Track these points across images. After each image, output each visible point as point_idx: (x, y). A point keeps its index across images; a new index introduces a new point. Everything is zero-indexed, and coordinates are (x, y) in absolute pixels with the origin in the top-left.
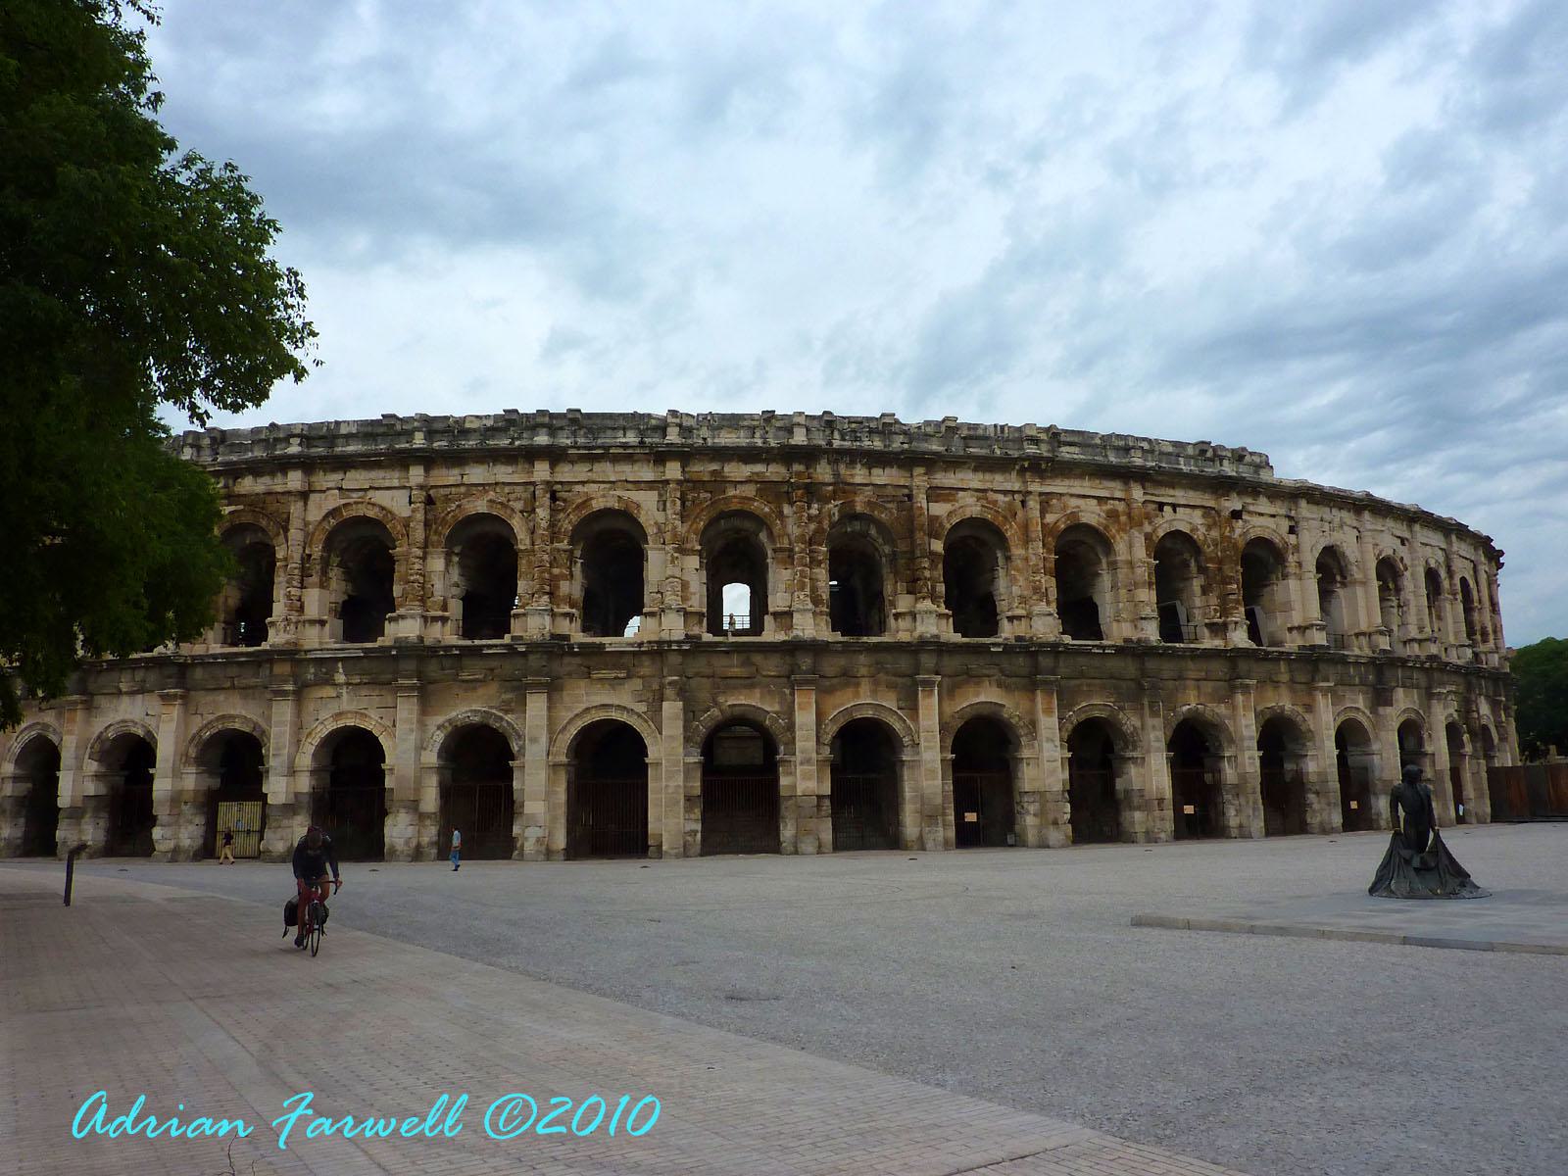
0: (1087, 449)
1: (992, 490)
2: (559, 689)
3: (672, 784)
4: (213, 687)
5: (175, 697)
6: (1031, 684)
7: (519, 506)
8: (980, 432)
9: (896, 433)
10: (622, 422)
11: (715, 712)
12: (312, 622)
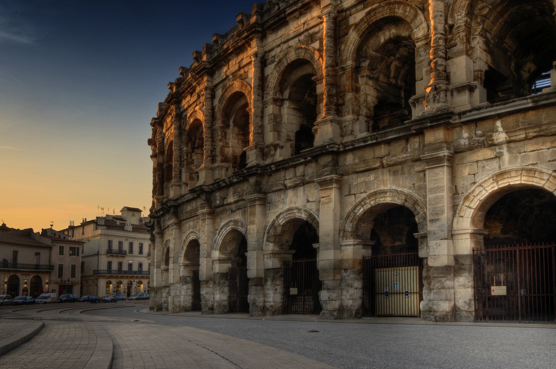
4: (364, 169)
5: (331, 181)
12: (460, 89)
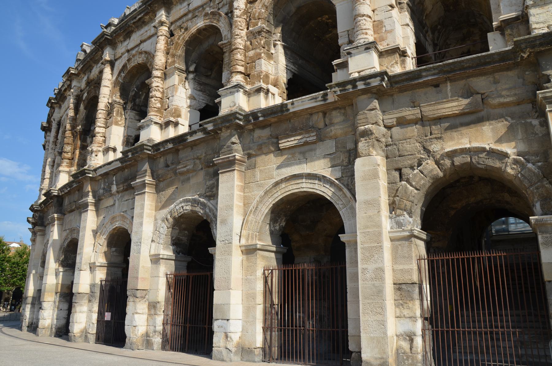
3: (371, 267)
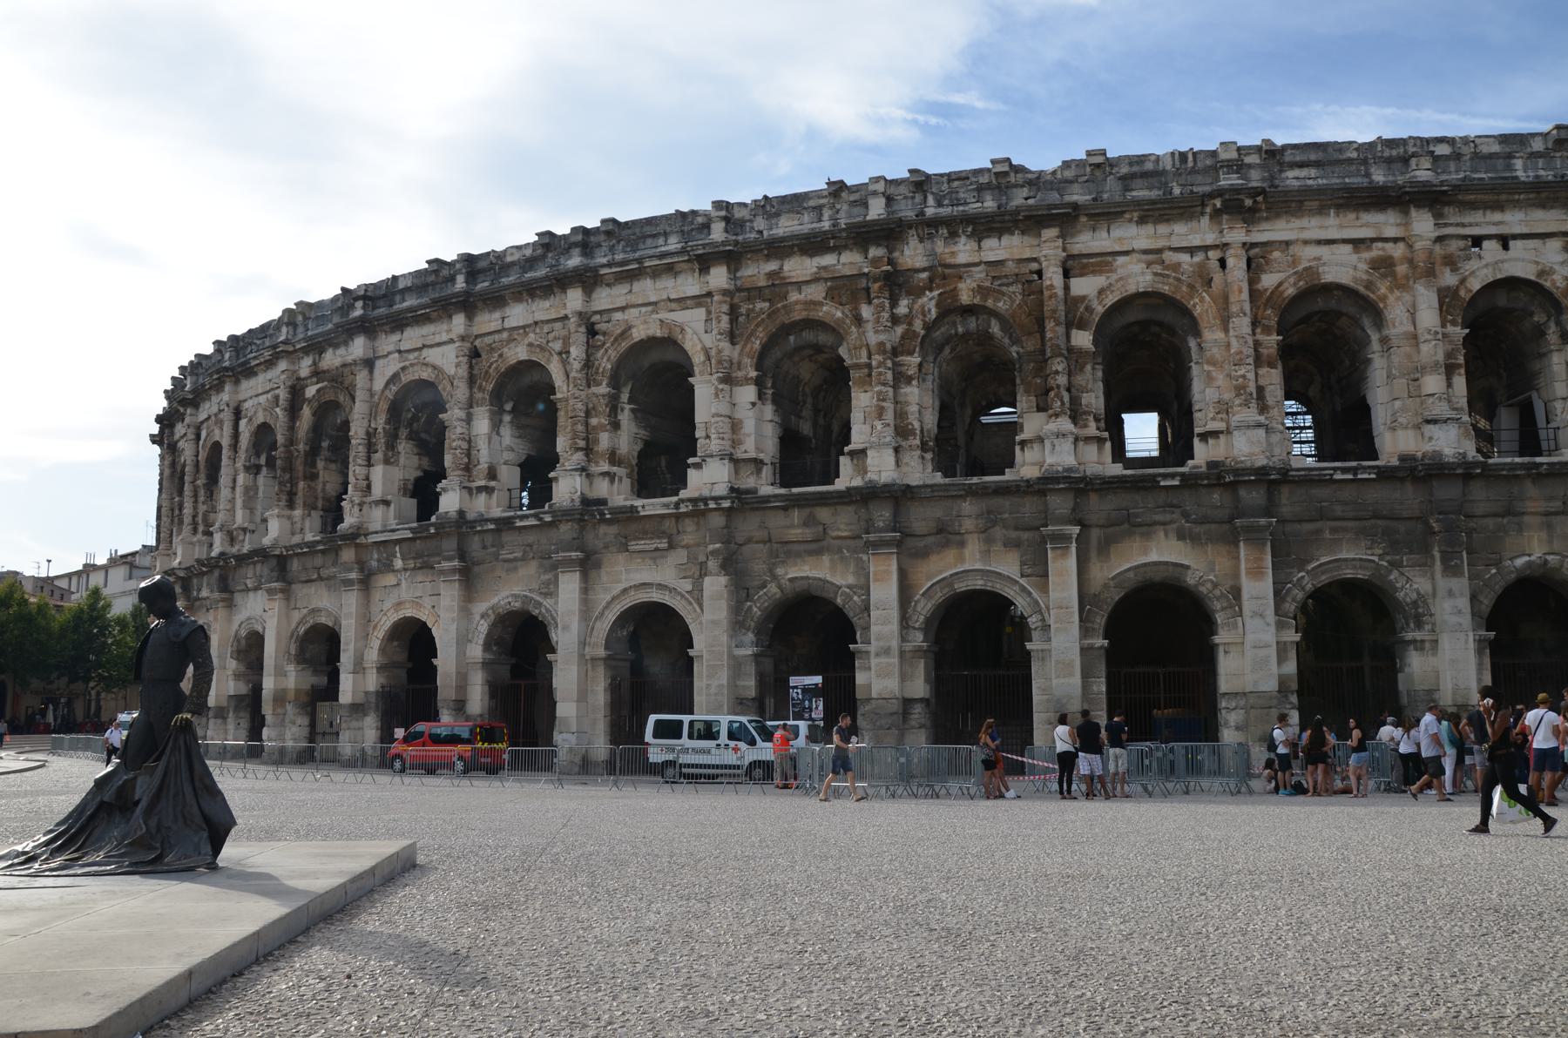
0: (1329, 169)
1: (1171, 249)
2: (598, 565)
3: (715, 683)
6: (1229, 532)
7: (557, 346)
8: (1149, 166)
9: (1016, 186)
10: (660, 229)
11: (773, 589)
12: (377, 503)
